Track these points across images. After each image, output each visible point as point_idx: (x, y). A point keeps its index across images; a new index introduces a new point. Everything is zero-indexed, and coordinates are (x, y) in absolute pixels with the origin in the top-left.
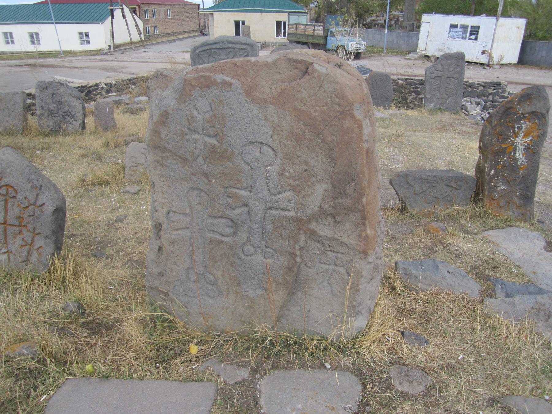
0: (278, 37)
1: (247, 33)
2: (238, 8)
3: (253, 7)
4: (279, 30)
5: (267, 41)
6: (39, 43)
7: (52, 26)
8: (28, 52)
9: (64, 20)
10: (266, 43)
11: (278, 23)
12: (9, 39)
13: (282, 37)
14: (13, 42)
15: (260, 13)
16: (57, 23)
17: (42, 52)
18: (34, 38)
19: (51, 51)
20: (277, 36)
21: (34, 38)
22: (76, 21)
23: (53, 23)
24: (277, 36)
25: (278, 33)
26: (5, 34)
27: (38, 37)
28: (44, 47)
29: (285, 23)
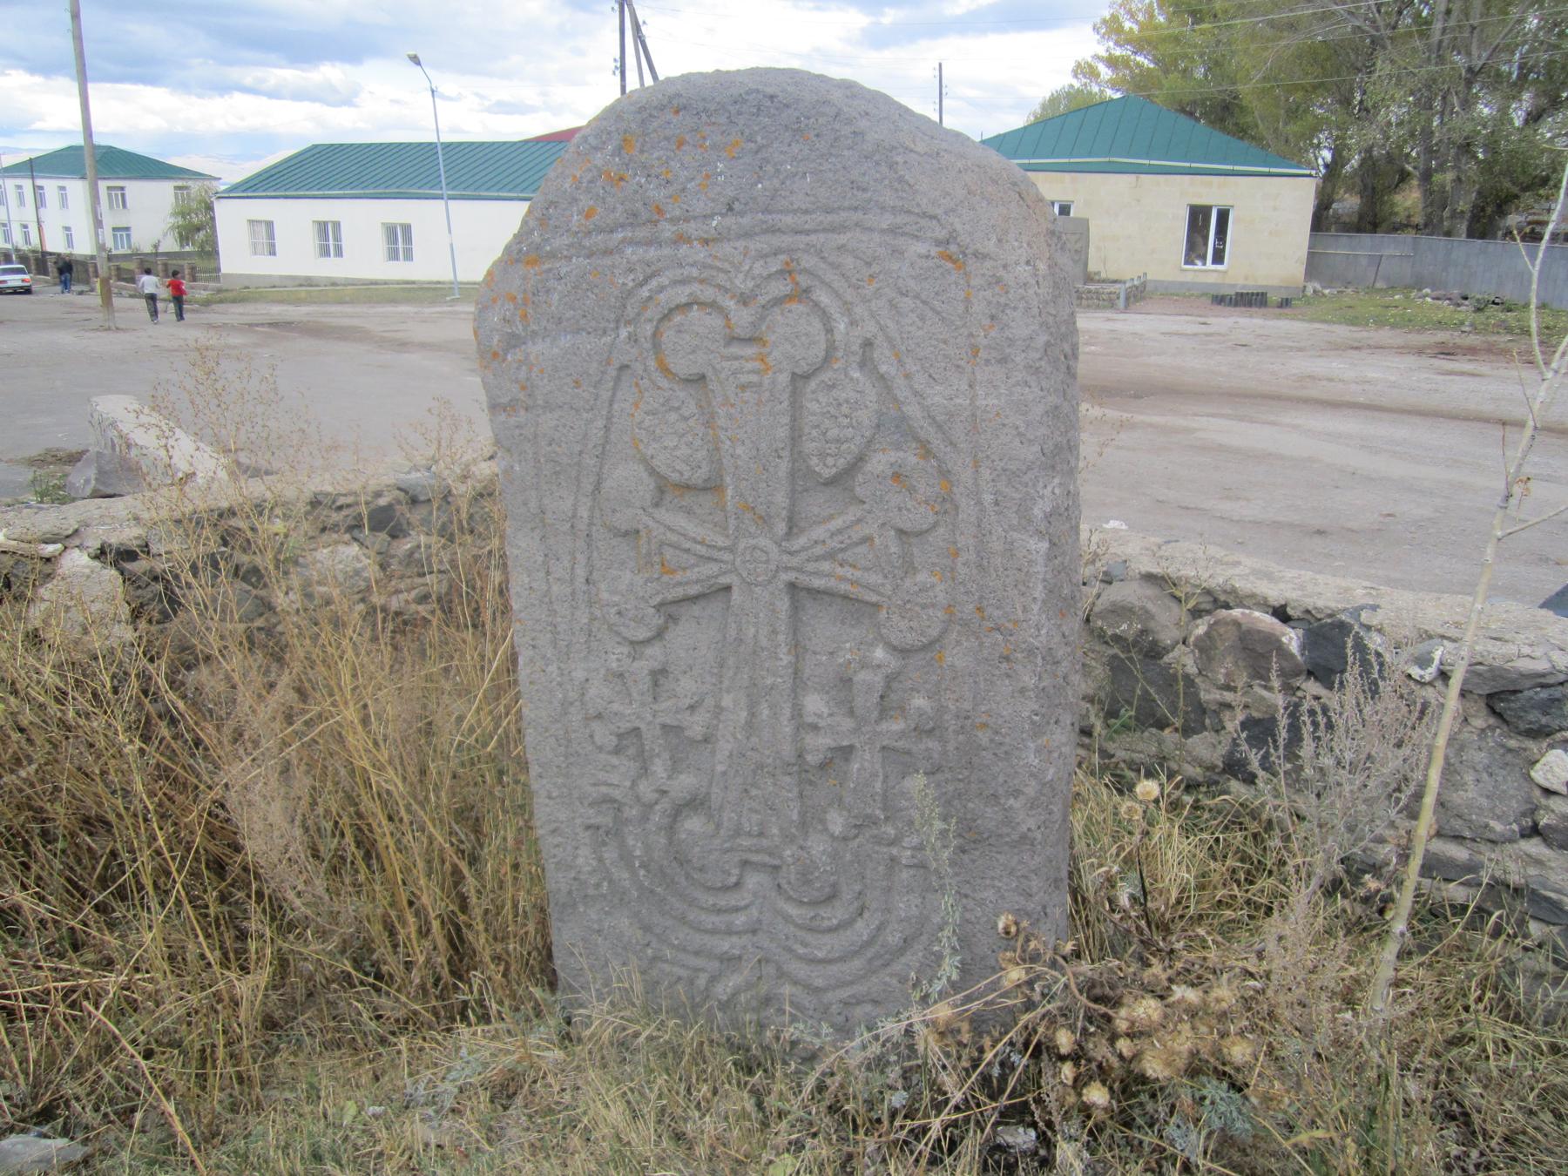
0: (1192, 263)
1: (1078, 246)
2: (1052, 155)
3: (1109, 153)
4: (1199, 240)
5: (1149, 277)
6: (409, 256)
7: (439, 205)
8: (375, 283)
9: (488, 189)
10: (1144, 284)
11: (1198, 217)
12: (331, 242)
13: (1209, 265)
14: (339, 252)
15: (1133, 177)
16: (451, 198)
17: (413, 282)
18: (398, 240)
19: (439, 283)
20: (1188, 261)
21: (398, 240)
22: (522, 191)
23: (440, 197)
24: (1188, 261)
25: (1194, 250)
26: (322, 228)
27: (408, 238)
28: (426, 266)
29: (1223, 216)
